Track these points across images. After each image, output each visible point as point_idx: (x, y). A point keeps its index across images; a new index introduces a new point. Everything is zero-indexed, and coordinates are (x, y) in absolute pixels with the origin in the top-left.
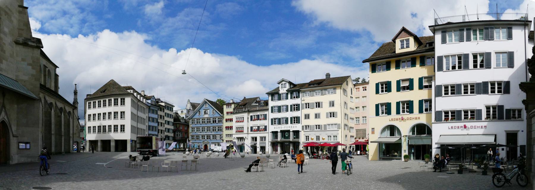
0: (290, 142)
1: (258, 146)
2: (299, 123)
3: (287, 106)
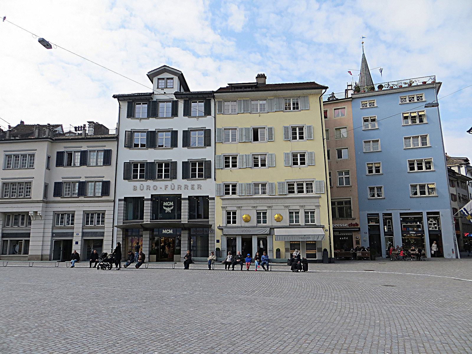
0: (184, 227)
3: (174, 134)
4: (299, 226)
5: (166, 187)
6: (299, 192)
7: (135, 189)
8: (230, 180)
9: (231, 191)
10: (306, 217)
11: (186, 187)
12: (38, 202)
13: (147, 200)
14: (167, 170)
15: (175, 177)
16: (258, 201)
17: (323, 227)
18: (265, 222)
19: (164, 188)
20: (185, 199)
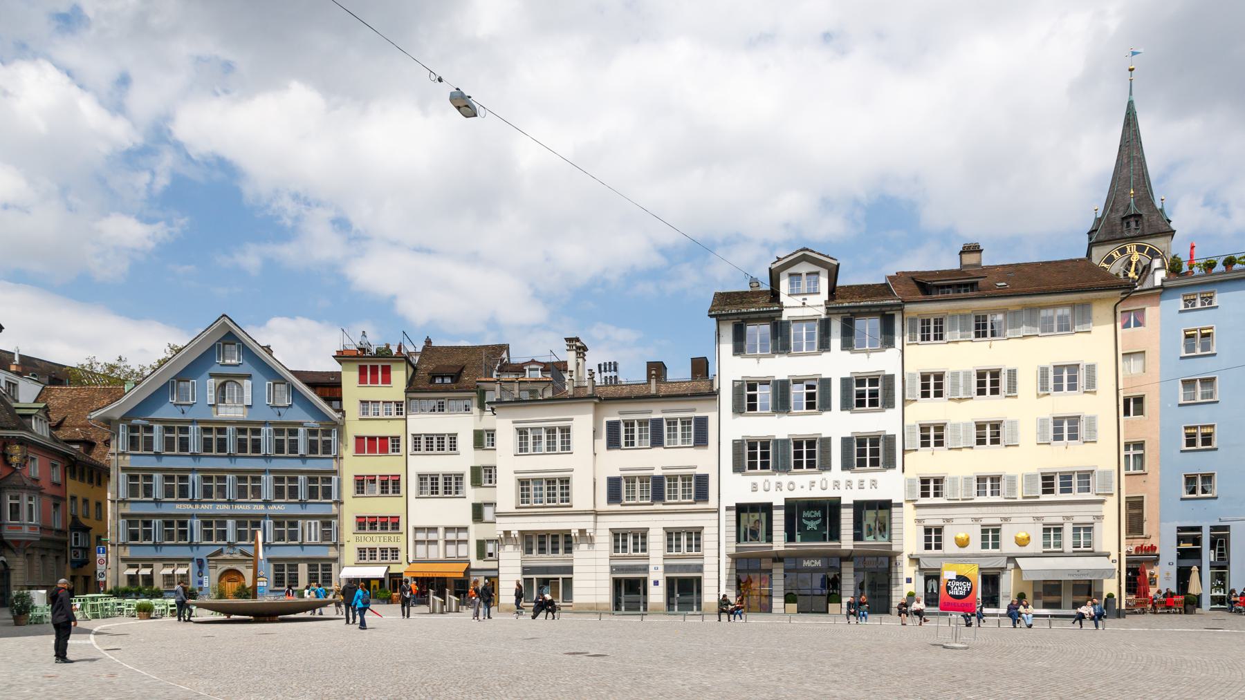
1: (656, 576)
2: (890, 464)
4: (1061, 554)
5: (812, 484)
6: (1062, 491)
7: (755, 488)
8: (931, 472)
9: (932, 491)
10: (1076, 537)
11: (849, 484)
12: (585, 513)
13: (778, 508)
14: (809, 453)
15: (826, 466)
16: (984, 509)
17: (1108, 556)
18: (996, 546)
19: (807, 486)
20: (847, 506)
